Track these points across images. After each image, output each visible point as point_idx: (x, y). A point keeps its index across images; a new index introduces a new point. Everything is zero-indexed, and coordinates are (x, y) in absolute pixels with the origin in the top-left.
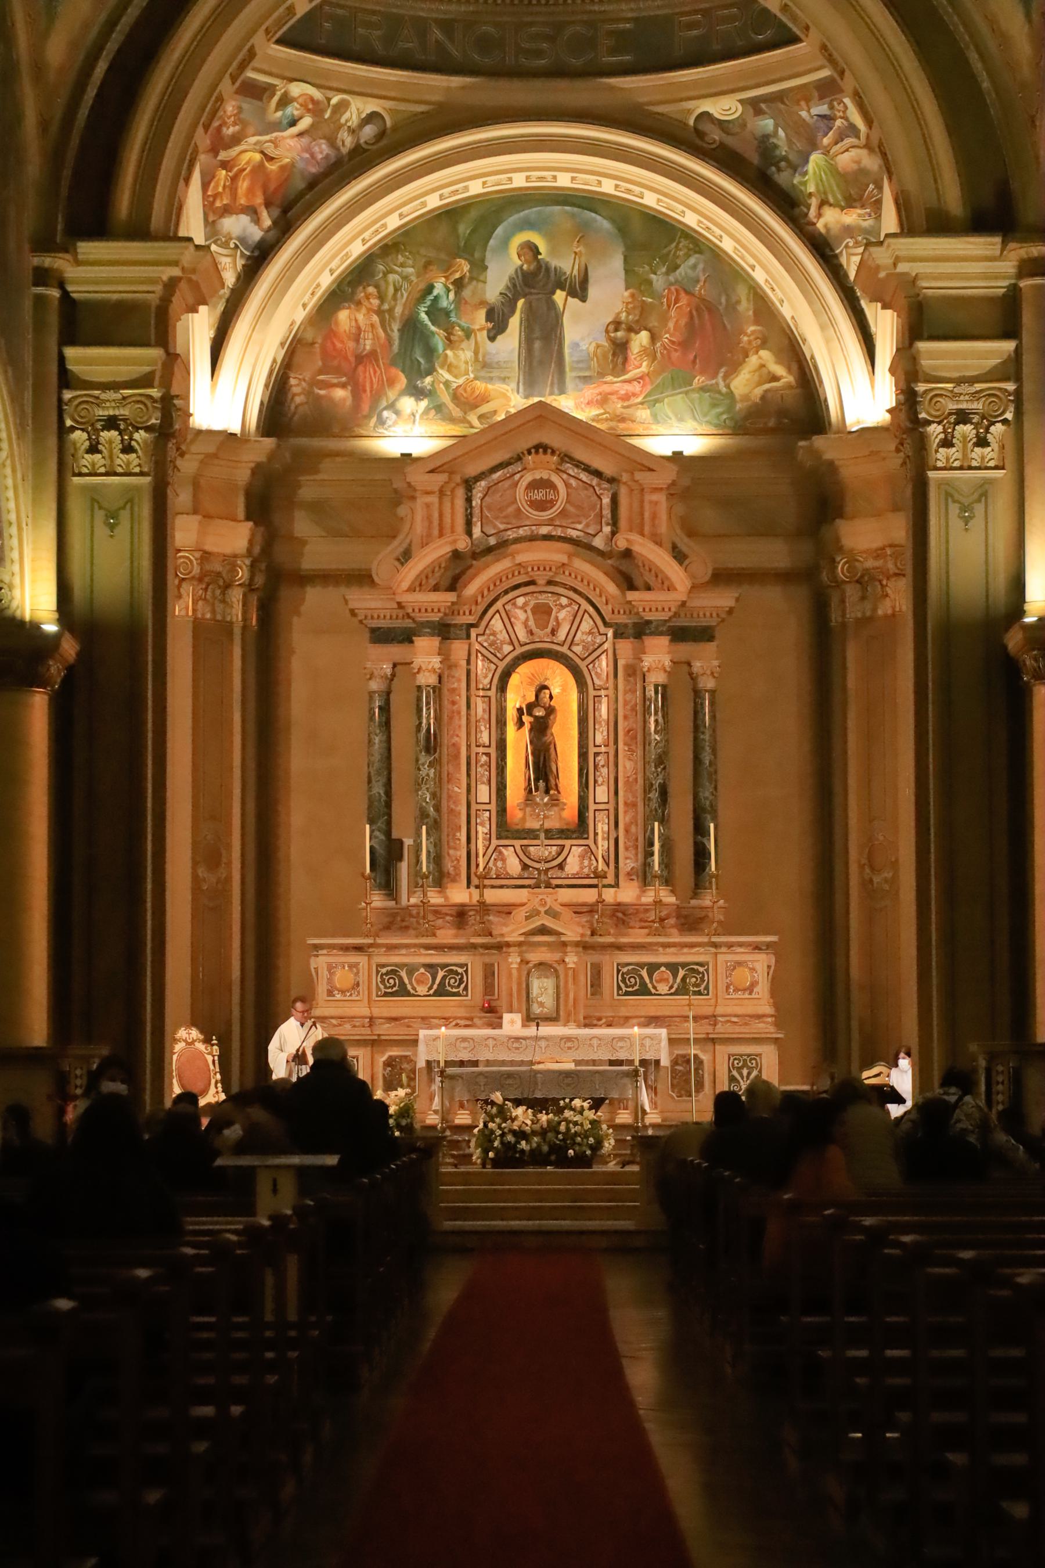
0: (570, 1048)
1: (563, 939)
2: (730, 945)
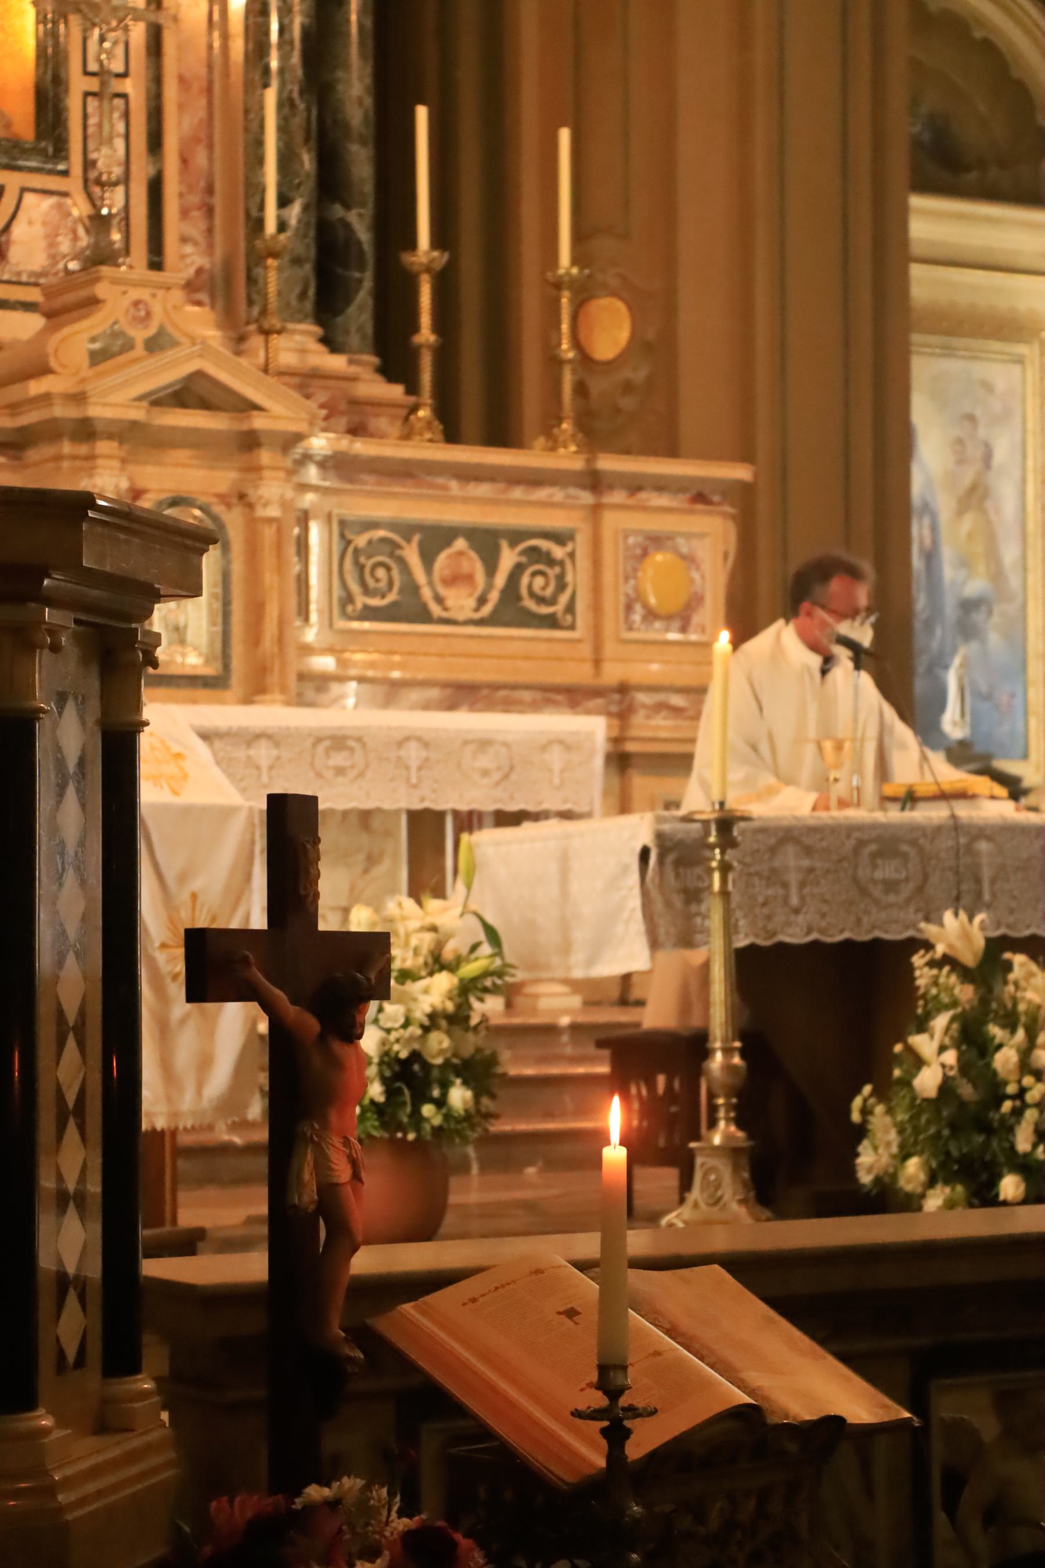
0: (340, 771)
1: (259, 422)
2: (635, 485)
